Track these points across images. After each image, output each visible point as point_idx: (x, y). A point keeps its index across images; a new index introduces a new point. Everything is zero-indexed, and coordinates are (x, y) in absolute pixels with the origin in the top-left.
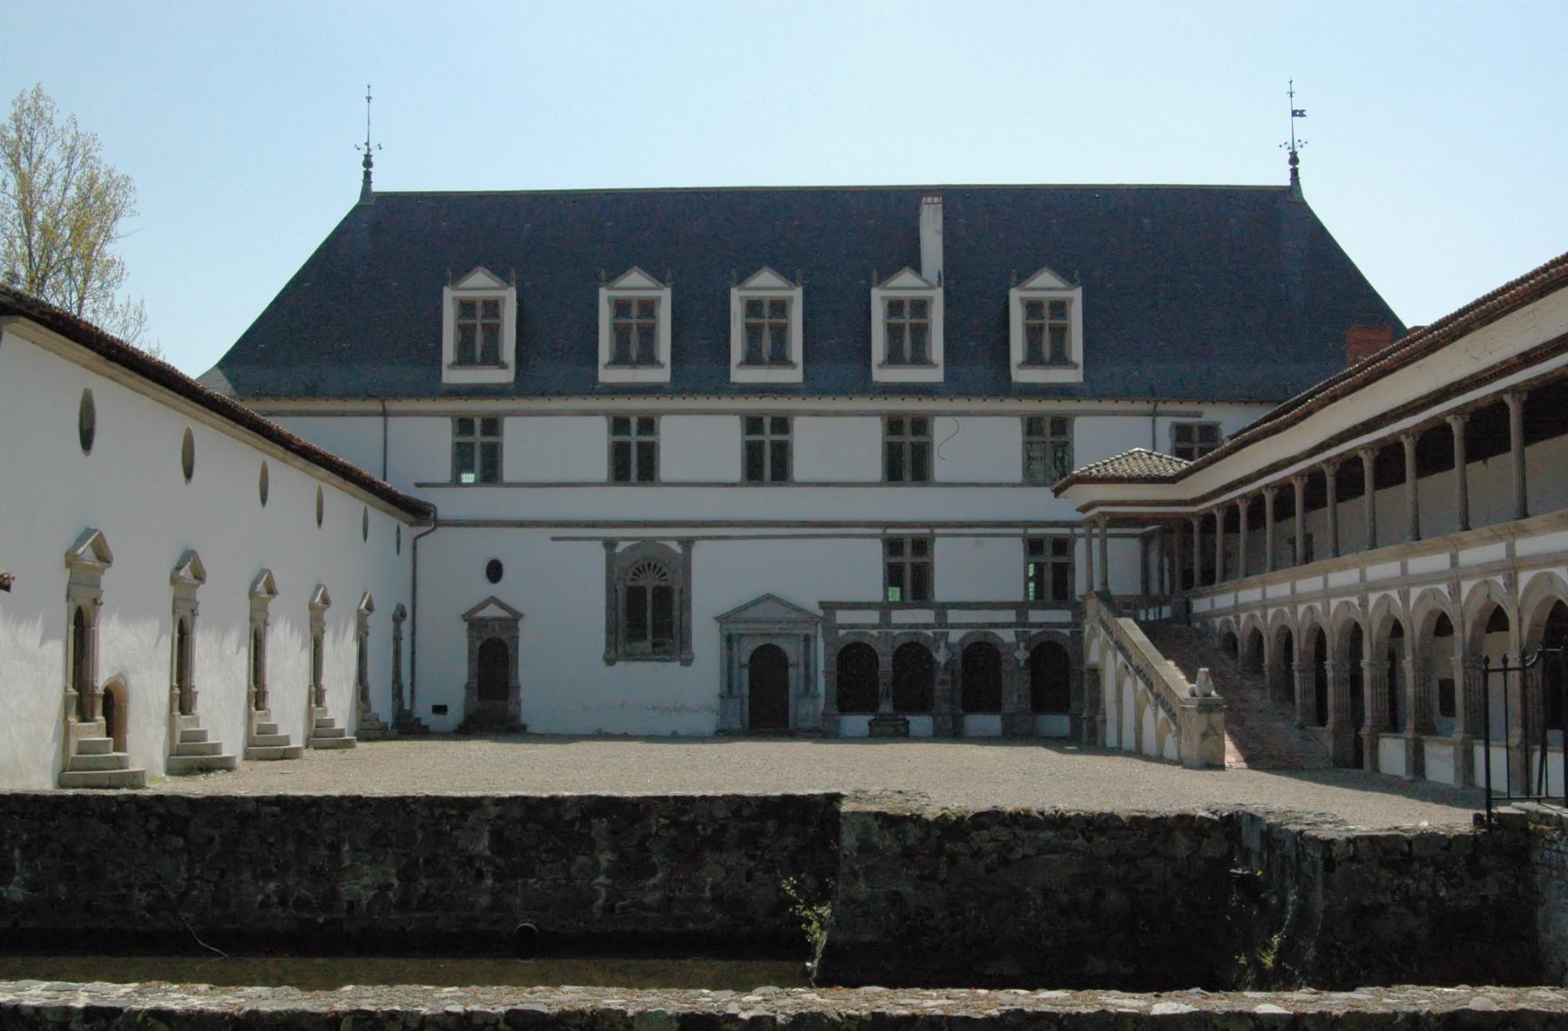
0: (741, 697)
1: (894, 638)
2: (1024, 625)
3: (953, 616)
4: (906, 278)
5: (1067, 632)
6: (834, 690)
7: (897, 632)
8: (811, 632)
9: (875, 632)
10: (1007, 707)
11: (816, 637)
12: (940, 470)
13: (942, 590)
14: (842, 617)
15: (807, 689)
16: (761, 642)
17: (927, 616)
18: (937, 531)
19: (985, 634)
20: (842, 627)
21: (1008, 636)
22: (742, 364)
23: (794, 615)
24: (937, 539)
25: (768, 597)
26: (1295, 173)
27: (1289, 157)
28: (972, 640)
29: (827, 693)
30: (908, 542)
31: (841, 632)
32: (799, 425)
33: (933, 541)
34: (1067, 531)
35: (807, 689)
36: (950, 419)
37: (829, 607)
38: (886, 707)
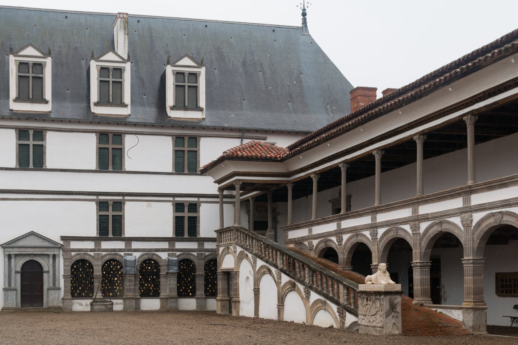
0: (16, 290)
2: (173, 250)
3: (135, 245)
4: (110, 56)
5: (195, 254)
6: (69, 285)
7: (104, 253)
8: (56, 253)
9: (92, 253)
10: (163, 294)
11: (59, 256)
12: (128, 165)
13: (128, 232)
14: (74, 245)
15: (54, 284)
16: (27, 259)
17: (120, 245)
18: (126, 198)
21: (164, 256)
22: (15, 101)
23: (46, 244)
24: (127, 203)
25: (32, 234)
26: (305, 22)
27: (301, 12)
28: (146, 257)
29: (65, 286)
30: (111, 203)
31: (73, 254)
32: (50, 136)
33: (124, 203)
34: (196, 199)
35: (54, 284)
36: (134, 136)
37: (66, 239)
38: (99, 295)
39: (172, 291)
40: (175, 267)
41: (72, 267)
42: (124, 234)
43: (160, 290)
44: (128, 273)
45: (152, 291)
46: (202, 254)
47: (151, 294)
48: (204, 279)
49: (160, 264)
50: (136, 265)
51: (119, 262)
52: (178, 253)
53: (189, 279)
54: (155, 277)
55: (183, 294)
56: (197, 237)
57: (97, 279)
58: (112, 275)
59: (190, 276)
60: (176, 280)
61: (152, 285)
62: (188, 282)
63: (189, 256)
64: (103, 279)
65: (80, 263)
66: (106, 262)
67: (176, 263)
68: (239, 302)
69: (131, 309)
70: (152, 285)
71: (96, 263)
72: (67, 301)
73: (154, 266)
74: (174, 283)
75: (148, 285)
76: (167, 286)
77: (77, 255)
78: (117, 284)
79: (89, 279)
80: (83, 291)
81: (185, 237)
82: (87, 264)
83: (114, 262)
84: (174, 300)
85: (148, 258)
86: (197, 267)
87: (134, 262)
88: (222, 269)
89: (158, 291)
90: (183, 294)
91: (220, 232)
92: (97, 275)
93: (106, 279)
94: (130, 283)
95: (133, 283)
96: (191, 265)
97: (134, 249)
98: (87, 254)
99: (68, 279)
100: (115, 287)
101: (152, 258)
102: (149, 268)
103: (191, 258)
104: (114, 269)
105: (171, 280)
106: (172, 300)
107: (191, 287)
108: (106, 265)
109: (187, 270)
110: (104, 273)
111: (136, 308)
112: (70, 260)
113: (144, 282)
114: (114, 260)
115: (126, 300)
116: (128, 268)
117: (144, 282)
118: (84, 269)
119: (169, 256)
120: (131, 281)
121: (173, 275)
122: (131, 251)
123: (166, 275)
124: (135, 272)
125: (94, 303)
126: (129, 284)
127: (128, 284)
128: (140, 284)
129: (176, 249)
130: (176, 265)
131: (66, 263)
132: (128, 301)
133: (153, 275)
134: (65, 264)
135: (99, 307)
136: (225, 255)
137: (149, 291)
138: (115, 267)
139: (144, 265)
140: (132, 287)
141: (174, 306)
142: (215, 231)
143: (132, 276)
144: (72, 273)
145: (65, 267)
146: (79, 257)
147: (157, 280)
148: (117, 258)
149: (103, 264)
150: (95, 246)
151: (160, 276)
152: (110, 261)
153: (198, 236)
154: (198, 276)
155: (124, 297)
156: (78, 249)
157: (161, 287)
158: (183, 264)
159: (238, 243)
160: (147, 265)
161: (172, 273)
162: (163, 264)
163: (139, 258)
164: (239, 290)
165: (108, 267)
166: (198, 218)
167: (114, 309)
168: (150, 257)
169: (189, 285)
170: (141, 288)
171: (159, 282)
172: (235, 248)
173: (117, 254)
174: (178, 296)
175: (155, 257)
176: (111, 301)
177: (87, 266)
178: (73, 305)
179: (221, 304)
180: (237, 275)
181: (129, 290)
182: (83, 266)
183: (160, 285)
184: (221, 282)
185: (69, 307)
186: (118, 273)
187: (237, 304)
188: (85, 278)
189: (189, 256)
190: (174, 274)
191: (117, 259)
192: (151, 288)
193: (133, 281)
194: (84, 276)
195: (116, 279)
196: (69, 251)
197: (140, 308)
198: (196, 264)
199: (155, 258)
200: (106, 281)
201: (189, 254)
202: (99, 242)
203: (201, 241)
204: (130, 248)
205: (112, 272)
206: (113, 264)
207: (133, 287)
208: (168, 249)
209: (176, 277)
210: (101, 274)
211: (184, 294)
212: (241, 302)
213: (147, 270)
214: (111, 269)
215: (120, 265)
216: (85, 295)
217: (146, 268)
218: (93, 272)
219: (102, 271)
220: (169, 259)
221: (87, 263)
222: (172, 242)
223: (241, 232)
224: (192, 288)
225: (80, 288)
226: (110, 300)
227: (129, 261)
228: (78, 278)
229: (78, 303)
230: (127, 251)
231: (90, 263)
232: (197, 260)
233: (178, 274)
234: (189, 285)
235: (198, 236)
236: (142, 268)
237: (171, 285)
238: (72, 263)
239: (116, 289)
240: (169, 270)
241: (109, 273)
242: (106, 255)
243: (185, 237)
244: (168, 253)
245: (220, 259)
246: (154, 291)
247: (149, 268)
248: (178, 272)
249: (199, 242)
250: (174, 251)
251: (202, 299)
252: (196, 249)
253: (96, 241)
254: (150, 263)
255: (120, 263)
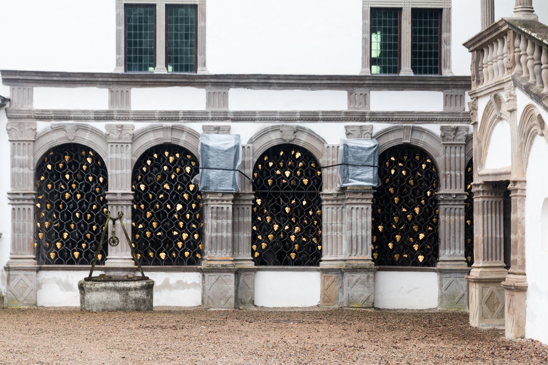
1: (135, 138)
2: (362, 117)
5: (435, 128)
6: (29, 224)
7: (139, 126)
9: (101, 126)
19: (297, 130)
20: (43, 116)
28: (274, 139)
31: (42, 126)
39: (355, 247)
40: (366, 169)
41: (40, 169)
42: (204, 65)
43: (321, 245)
44: (212, 189)
45: (297, 246)
46: (457, 129)
47: (293, 255)
48: (463, 211)
49: (322, 161)
50: (239, 163)
51: (188, 152)
52: (379, 127)
53: (417, 210)
54: (304, 203)
55: (397, 256)
56: (441, 74)
57: (117, 206)
58: (166, 196)
59: (419, 200)
60: (370, 212)
61: (297, 229)
62: (413, 218)
63: (416, 136)
64: (139, 206)
65: (67, 158)
66: (147, 154)
67: (370, 157)
68: (522, 289)
69: (222, 303)
70: (297, 229)
71: (114, 156)
72: (21, 274)
73: (303, 167)
74: (364, 220)
75: (280, 227)
76: (341, 230)
77: (56, 129)
78: (181, 224)
79: (94, 207)
80: (74, 244)
81: (402, 74)
82: (89, 160)
83: (172, 154)
84: (363, 276)
85: (281, 142)
86: (442, 173)
87: (233, 153)
88: (490, 172)
89: (314, 246)
90: (397, 256)
91: (477, 45)
92: (116, 194)
93: (146, 205)
94: (219, 221)
95: (230, 221)
96: (424, 166)
97: (236, 113)
98: (85, 129)
99: (27, 207)
100: (175, 233)
101: (294, 143)
102: (287, 173)
103: (423, 141)
104: (173, 176)
105: (354, 211)
106: (357, 276)
107: (422, 236)
108: (149, 162)
109: (411, 182)
110: (142, 187)
111: (238, 301)
112: (31, 147)
113: (268, 219)
114: (173, 148)
115: (206, 275)
116: (212, 174)
117: (268, 219)
118: (79, 176)
119: (348, 134)
120: (222, 213)
121: (359, 196)
122: (226, 119)
123: (340, 197)
124: (234, 184)
125: (88, 285)
126: (214, 222)
127: (210, 222)
128: (254, 221)
129: (373, 114)
130: (371, 163)
131: (19, 155)
132: (211, 278)
133: (300, 196)
134: (16, 157)
135: (103, 296)
136: (493, 126)
137: (285, 247)
138: (178, 170)
139: (271, 164)
140: (225, 235)
141: (362, 295)
142: (464, 45)
143: (225, 198)
144: (40, 188)
145: (16, 169)
146: (62, 138)
147: (311, 213)
148: (183, 140)
149: (136, 159)
150: (112, 102)
151: (320, 201)
152: (160, 148)
153: (446, 73)
154: (443, 200)
155: (204, 265)
156: (55, 112)
157: (325, 233)
158: (396, 162)
159: (518, 79)
160: (281, 164)
161: (356, 191)
162: (330, 159)
163: (251, 141)
164: (523, 248)
165: (155, 169)
166: (444, 13)
167: (155, 304)
168: (288, 137)
169: (415, 228)
170: (260, 237)
171: (319, 218)
172: (513, 98)
173: (181, 130)
174: (375, 265)
175: (303, 140)
176: (144, 278)
177: (88, 164)
178: (43, 287)
179: (482, 295)
180: (519, 193)
181: (218, 243)
182: (76, 165)
183: (321, 228)
184: (481, 216)
185: (26, 294)
186: (185, 188)
187: (518, 296)
188: (81, 204)
189: (416, 136)
190: (363, 193)
191: (181, 144)
192: (293, 238)
193: (227, 213)
194: (79, 196)
195: (179, 207)
196: (29, 117)
197: (253, 302)
198: (439, 161)
199: (305, 143)
200: (149, 214)
201: (413, 129)
202: (125, 89)
203: (456, 87)
204: (223, 109)
205: (167, 186)
206: (171, 159)
207: (230, 235)
208: (346, 113)
209: (369, 201)
210: (130, 191)
211: (401, 256)
212: (529, 289)
213: (279, 181)
214: (165, 177)
215: (193, 164)
216: (80, 256)
217: (278, 172)
218: (105, 184)
219: (134, 180)
220: (346, 146)
221: (88, 155)
222: (358, 91)
223: (527, 38)
224: (424, 239)
225: (65, 235)
226: (139, 274)
227: (217, 151)
228: (59, 203)
229: (59, 282)
230: (213, 119)
231: (97, 157)
232: (441, 149)
233: (374, 194)
234: (415, 228)
235: (446, 73)
236: (265, 173)
237: (354, 227)
238: (39, 155)
239: (181, 240)
240: (345, 178)
241: (155, 188)
242: (145, 132)
243: (402, 74)
244: (346, 127)
245: (479, 142)
246: (300, 249)
247: (287, 173)
248: (375, 185)
249: (449, 92)
250: (365, 120)
251: (458, 275)
252: (437, 113)
253: (116, 88)
254: (288, 156)
255: (194, 159)
